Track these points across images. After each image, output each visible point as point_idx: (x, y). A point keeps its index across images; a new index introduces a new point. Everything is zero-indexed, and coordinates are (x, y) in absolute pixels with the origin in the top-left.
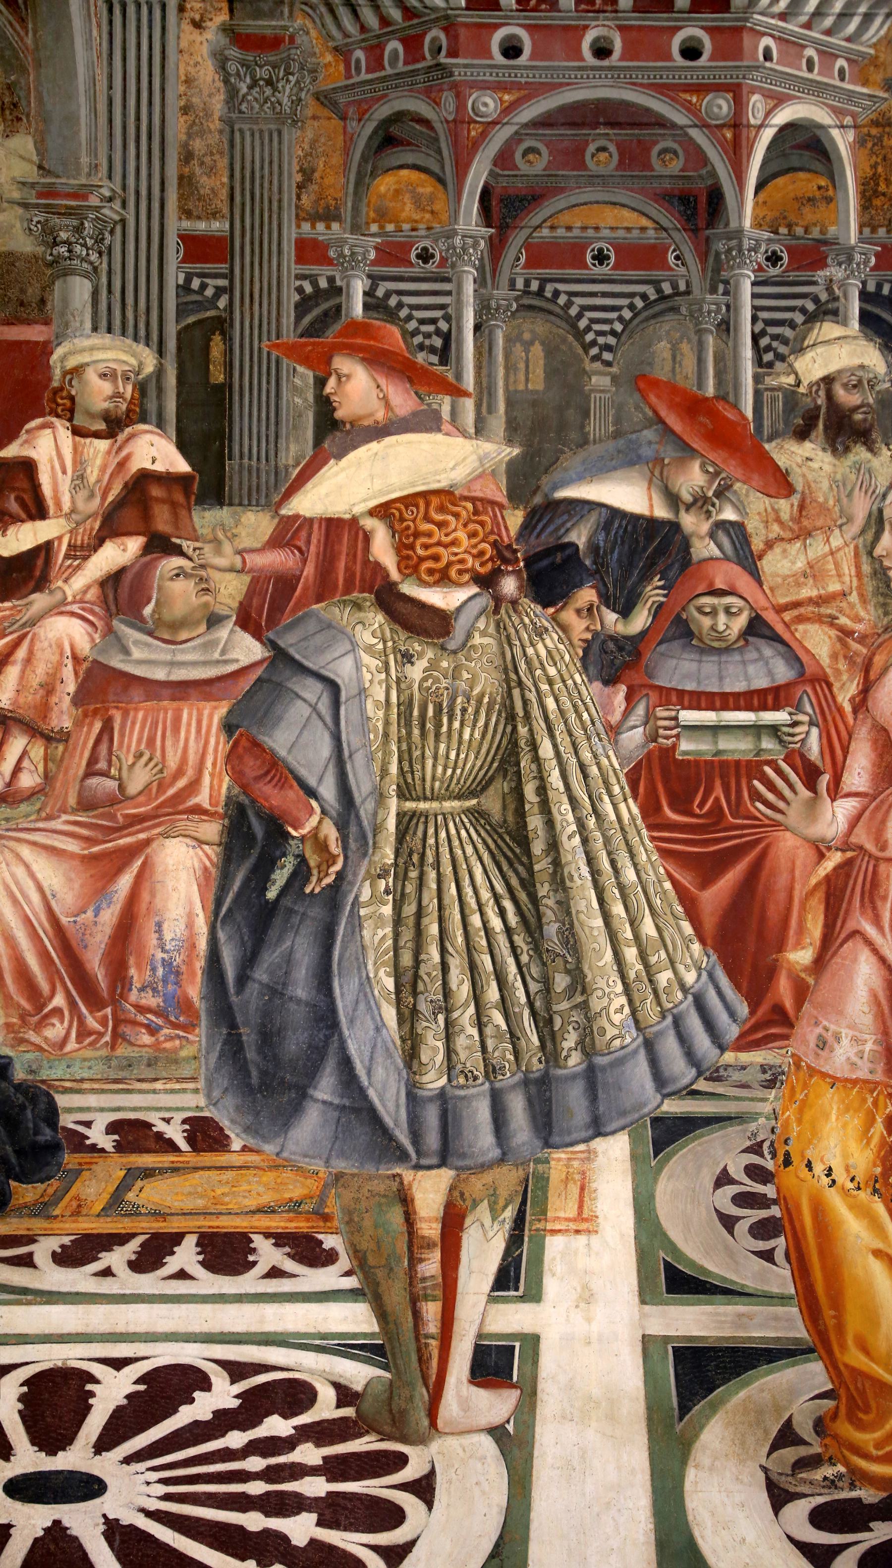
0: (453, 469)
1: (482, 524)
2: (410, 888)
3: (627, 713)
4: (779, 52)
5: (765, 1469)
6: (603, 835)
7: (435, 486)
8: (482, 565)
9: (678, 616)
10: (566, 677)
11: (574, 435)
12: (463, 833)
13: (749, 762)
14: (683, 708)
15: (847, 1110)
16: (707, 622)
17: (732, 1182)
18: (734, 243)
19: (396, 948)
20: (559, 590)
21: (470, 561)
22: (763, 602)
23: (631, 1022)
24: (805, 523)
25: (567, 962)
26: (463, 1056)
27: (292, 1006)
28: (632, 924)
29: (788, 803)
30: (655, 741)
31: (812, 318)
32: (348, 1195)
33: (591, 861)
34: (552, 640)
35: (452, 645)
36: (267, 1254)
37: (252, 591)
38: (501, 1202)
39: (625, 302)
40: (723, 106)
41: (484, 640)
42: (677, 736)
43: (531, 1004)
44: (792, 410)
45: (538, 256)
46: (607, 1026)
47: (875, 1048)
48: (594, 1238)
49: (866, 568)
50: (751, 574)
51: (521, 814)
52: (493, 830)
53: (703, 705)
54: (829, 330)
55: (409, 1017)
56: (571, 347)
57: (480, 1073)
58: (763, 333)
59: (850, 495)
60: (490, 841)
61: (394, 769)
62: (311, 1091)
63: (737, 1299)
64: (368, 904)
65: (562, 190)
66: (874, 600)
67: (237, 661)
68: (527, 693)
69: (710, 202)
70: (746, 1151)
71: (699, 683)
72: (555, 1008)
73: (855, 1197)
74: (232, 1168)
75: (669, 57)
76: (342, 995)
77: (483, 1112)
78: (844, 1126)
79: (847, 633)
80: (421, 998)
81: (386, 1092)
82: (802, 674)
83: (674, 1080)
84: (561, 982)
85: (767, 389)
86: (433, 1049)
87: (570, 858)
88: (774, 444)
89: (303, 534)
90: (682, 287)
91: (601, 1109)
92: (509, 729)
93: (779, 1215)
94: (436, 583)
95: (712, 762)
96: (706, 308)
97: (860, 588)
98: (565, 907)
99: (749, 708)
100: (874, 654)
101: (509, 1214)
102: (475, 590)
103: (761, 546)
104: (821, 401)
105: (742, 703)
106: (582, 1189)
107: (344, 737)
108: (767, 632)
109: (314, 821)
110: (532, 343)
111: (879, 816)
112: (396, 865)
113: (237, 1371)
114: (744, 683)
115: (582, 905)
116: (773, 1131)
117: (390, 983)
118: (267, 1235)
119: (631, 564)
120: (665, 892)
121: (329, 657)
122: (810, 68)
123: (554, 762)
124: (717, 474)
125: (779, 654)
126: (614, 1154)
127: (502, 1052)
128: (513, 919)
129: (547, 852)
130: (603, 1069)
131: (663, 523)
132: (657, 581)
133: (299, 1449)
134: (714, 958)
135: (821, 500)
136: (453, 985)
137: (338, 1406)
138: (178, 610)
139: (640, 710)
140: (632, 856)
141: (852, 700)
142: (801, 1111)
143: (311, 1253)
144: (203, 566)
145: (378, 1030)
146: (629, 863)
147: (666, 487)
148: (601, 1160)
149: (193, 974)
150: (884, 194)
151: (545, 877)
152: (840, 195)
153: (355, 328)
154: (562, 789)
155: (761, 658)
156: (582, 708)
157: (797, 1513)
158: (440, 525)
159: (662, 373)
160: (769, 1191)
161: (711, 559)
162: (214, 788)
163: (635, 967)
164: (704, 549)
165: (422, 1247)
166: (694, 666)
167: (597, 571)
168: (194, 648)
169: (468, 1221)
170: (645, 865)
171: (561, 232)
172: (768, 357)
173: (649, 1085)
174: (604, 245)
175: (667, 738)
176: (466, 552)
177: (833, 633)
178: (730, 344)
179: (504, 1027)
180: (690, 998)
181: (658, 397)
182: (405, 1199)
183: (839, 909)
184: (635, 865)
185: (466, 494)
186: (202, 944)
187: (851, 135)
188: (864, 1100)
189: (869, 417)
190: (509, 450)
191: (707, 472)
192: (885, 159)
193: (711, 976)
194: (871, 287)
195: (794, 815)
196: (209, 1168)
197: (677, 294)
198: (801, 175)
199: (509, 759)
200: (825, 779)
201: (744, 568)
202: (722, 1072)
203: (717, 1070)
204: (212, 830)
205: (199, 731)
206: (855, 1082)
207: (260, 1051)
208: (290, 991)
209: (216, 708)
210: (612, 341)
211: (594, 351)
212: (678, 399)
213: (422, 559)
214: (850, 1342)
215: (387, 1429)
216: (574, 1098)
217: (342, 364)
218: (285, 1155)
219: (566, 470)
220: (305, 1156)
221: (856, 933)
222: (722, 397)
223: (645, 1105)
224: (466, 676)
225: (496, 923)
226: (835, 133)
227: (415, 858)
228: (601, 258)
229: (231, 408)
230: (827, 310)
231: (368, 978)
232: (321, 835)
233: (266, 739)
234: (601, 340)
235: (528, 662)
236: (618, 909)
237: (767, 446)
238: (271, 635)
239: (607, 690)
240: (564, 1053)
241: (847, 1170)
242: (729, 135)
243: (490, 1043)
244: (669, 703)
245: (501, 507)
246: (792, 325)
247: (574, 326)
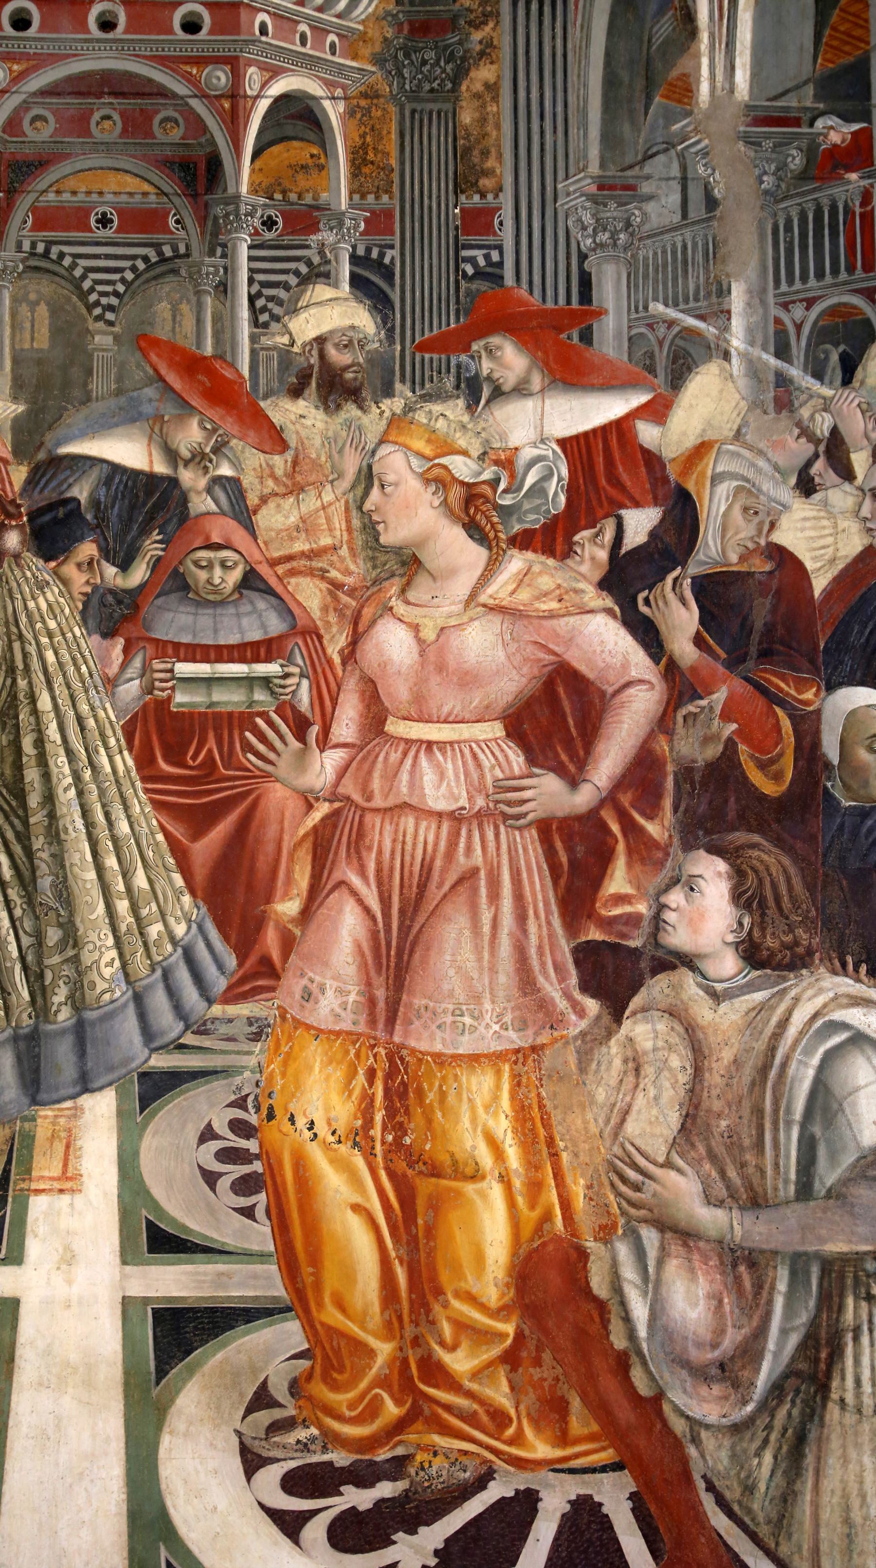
3: (124, 666)
4: (274, 27)
5: (239, 1434)
6: (98, 787)
9: (176, 571)
10: (66, 630)
11: (77, 393)
14: (179, 661)
15: (330, 1062)
16: (203, 575)
17: (216, 1137)
18: (231, 208)
20: (61, 544)
22: (257, 556)
23: (121, 975)
24: (299, 478)
25: (59, 915)
28: (125, 875)
29: (279, 755)
30: (151, 693)
31: (305, 281)
34: (53, 593)
39: (127, 264)
40: (221, 77)
42: (173, 688)
43: (22, 958)
44: (287, 368)
45: (44, 219)
46: (97, 980)
47: (358, 999)
48: (78, 1199)
49: (356, 523)
50: (246, 528)
51: (18, 767)
53: (198, 657)
54: (321, 291)
56: (75, 307)
58: (259, 295)
59: (341, 451)
63: (217, 1257)
65: (68, 156)
66: (363, 554)
68: (27, 646)
69: (208, 170)
71: (194, 636)
72: (47, 962)
73: (335, 1150)
75: (171, 31)
78: (327, 1079)
79: (337, 586)
82: (294, 627)
83: (163, 1033)
84: (53, 935)
87: (65, 810)
88: (269, 402)
90: (182, 250)
91: (90, 1064)
92: (9, 682)
93: (260, 1171)
95: (206, 714)
96: (204, 270)
97: (349, 542)
98: (59, 860)
99: (243, 660)
100: (362, 607)
103: (256, 501)
104: (314, 360)
105: (236, 654)
106: (68, 1147)
108: (262, 586)
110: (37, 303)
111: (366, 766)
114: (238, 636)
116: (257, 1085)
119: (130, 519)
120: (157, 844)
122: (303, 43)
123: (52, 715)
124: (215, 430)
125: (273, 607)
126: (101, 1108)
129: (43, 805)
130: (93, 1023)
131: (162, 478)
132: (156, 536)
134: (204, 909)
135: (314, 456)
139: (137, 662)
140: (126, 808)
141: (341, 652)
142: (285, 1063)
146: (123, 816)
148: (87, 1116)
150: (372, 163)
151: (41, 830)
152: (331, 163)
154: (59, 742)
155: (255, 610)
157: (270, 1477)
159: (162, 333)
160: (253, 1146)
161: (208, 513)
163: (126, 919)
164: (202, 504)
166: (190, 619)
167: (98, 526)
170: (139, 818)
171: (66, 196)
172: (264, 318)
173: (137, 1039)
174: (108, 209)
175: (163, 690)
177: (324, 586)
178: (228, 304)
180: (180, 951)
181: (158, 355)
183: (326, 859)
184: (129, 817)
187: (341, 106)
188: (347, 1052)
189: (360, 376)
190: (14, 407)
192: (372, 129)
193: (200, 928)
194: (361, 251)
195: (284, 766)
197: (177, 256)
198: (296, 144)
200: (315, 730)
201: (240, 522)
202: (209, 1026)
203: (204, 1024)
206: (338, 1034)
210: (114, 301)
211: (98, 311)
212: (177, 359)
214: (327, 1300)
219: (69, 426)
221: (342, 883)
222: (219, 357)
223: (133, 1059)
226: (327, 104)
228: (104, 221)
230: (320, 273)
234: (104, 301)
235: (29, 616)
236: (111, 862)
237: (262, 404)
239: (106, 643)
240: (54, 1008)
241: (329, 1123)
242: (227, 105)
244: (165, 655)
246: (287, 287)
247: (79, 287)
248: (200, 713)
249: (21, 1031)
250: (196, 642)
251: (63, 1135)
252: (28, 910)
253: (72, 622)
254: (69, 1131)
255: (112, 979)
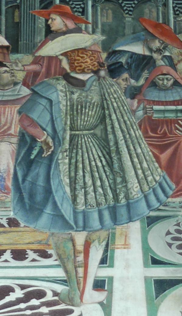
0: (86, 43)
1: (94, 57)
2: (74, 155)
3: (138, 107)
6: (131, 140)
7: (81, 47)
8: (95, 68)
12: (89, 140)
13: (174, 120)
14: (154, 105)
16: (161, 82)
17: (171, 234)
19: (70, 171)
21: (91, 67)
23: (140, 190)
25: (120, 174)
26: (89, 200)
27: (39, 187)
32: (56, 239)
33: (128, 147)
35: (86, 89)
36: (31, 255)
37: (27, 76)
38: (102, 240)
41: (95, 88)
42: (153, 113)
46: (133, 192)
50: (174, 69)
51: (107, 135)
52: (98, 139)
55: (73, 190)
57: (95, 205)
58: (176, 6)
60: (97, 142)
61: (69, 123)
62: (44, 210)
63: (173, 265)
64: (61, 159)
67: (22, 94)
68: (108, 102)
70: (175, 225)
71: (158, 99)
74: (20, 231)
76: (54, 184)
77: (96, 215)
80: (77, 185)
81: (67, 210)
84: (119, 180)
85: (177, 21)
86: (81, 199)
89: (42, 61)
92: (103, 111)
94: (81, 73)
95: (163, 120)
98: (120, 159)
99: (174, 105)
101: (104, 243)
102: (92, 74)
105: (172, 104)
107: (54, 114)
109: (45, 137)
112: (69, 149)
113: (23, 287)
115: (125, 159)
117: (68, 181)
118: (32, 250)
120: (149, 155)
121: (49, 93)
126: (136, 227)
127: (102, 199)
128: (104, 163)
129: (114, 145)
130: (132, 203)
131: (148, 56)
132: (146, 71)
133: (41, 308)
134: (165, 173)
136: (87, 181)
137: (53, 296)
138: (5, 81)
139: (142, 106)
140: (140, 145)
143: (44, 255)
144: (12, 70)
145: (64, 193)
147: (149, 47)
149: (9, 179)
151: (114, 151)
153: (57, 7)
156: (124, 106)
158: (82, 57)
159: (146, 17)
161: (162, 65)
162: (15, 129)
164: (160, 63)
165: (78, 253)
166: (157, 94)
168: (10, 91)
169: (91, 246)
170: (145, 148)
175: (150, 113)
176: (90, 64)
178: (166, 9)
179: (102, 192)
180: (158, 184)
182: (72, 240)
184: (141, 148)
185: (89, 49)
186: (12, 171)
190: (102, 37)
191: (161, 43)
193: (164, 177)
196: (14, 232)
199: (103, 119)
202: (167, 204)
203: (166, 203)
204: (15, 140)
205: (11, 113)
207: (29, 200)
208: (38, 183)
209: (16, 107)
210: (131, 9)
211: (126, 12)
213: (77, 67)
215: (68, 303)
216: (123, 211)
217: (53, 16)
218: (37, 228)
220: (43, 228)
224: (90, 97)
225: (99, 164)
227: (75, 147)
229: (21, 28)
231: (61, 180)
232: (47, 141)
233: (30, 115)
234: (128, 9)
235: (108, 94)
236: (136, 160)
237: (177, 36)
238: (32, 87)
239: (132, 101)
240: (120, 199)
243: (98, 197)
245: (100, 52)
247: (121, 6)
248: (161, 120)
249: (111, 205)
250: (160, 100)
251: (124, 233)
252: (111, 173)
253: (121, 95)
254: (126, 232)
255: (137, 192)
